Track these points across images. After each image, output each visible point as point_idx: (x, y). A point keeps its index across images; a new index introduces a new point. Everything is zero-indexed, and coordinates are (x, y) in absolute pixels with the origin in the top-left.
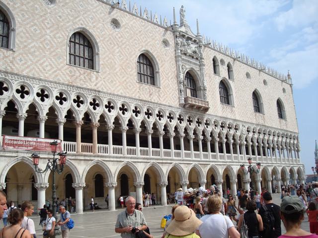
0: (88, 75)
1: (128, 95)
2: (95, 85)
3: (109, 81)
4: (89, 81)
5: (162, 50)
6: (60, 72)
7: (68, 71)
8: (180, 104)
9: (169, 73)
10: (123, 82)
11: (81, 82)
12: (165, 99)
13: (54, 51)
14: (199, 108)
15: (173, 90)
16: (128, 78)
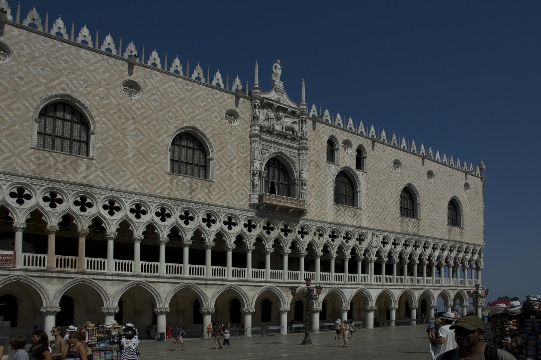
0: (71, 163)
1: (146, 191)
2: (85, 177)
3: (113, 171)
4: (73, 172)
5: (223, 127)
6: (18, 160)
7: (33, 158)
8: (250, 205)
9: (232, 160)
10: (140, 173)
11: (59, 173)
12: (219, 198)
13: (6, 129)
14: (286, 210)
15: (238, 185)
16: (149, 167)
